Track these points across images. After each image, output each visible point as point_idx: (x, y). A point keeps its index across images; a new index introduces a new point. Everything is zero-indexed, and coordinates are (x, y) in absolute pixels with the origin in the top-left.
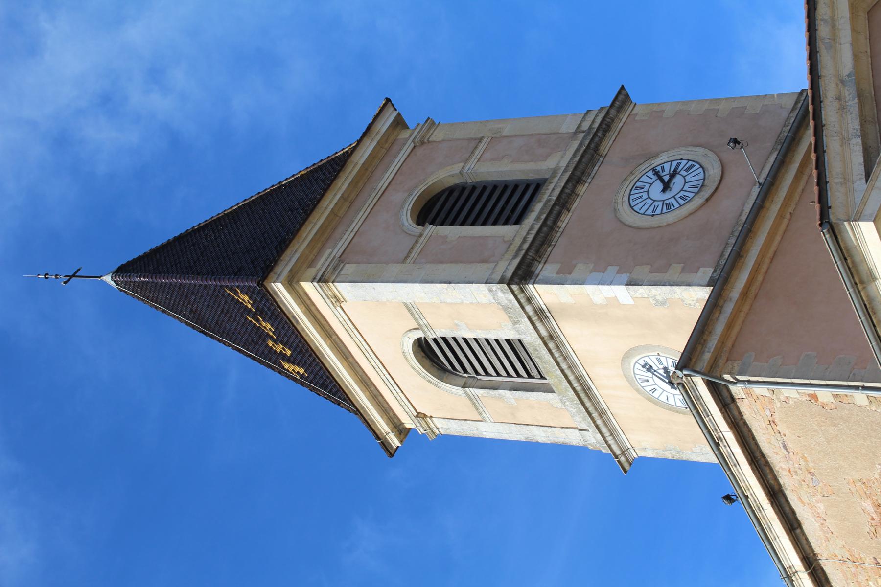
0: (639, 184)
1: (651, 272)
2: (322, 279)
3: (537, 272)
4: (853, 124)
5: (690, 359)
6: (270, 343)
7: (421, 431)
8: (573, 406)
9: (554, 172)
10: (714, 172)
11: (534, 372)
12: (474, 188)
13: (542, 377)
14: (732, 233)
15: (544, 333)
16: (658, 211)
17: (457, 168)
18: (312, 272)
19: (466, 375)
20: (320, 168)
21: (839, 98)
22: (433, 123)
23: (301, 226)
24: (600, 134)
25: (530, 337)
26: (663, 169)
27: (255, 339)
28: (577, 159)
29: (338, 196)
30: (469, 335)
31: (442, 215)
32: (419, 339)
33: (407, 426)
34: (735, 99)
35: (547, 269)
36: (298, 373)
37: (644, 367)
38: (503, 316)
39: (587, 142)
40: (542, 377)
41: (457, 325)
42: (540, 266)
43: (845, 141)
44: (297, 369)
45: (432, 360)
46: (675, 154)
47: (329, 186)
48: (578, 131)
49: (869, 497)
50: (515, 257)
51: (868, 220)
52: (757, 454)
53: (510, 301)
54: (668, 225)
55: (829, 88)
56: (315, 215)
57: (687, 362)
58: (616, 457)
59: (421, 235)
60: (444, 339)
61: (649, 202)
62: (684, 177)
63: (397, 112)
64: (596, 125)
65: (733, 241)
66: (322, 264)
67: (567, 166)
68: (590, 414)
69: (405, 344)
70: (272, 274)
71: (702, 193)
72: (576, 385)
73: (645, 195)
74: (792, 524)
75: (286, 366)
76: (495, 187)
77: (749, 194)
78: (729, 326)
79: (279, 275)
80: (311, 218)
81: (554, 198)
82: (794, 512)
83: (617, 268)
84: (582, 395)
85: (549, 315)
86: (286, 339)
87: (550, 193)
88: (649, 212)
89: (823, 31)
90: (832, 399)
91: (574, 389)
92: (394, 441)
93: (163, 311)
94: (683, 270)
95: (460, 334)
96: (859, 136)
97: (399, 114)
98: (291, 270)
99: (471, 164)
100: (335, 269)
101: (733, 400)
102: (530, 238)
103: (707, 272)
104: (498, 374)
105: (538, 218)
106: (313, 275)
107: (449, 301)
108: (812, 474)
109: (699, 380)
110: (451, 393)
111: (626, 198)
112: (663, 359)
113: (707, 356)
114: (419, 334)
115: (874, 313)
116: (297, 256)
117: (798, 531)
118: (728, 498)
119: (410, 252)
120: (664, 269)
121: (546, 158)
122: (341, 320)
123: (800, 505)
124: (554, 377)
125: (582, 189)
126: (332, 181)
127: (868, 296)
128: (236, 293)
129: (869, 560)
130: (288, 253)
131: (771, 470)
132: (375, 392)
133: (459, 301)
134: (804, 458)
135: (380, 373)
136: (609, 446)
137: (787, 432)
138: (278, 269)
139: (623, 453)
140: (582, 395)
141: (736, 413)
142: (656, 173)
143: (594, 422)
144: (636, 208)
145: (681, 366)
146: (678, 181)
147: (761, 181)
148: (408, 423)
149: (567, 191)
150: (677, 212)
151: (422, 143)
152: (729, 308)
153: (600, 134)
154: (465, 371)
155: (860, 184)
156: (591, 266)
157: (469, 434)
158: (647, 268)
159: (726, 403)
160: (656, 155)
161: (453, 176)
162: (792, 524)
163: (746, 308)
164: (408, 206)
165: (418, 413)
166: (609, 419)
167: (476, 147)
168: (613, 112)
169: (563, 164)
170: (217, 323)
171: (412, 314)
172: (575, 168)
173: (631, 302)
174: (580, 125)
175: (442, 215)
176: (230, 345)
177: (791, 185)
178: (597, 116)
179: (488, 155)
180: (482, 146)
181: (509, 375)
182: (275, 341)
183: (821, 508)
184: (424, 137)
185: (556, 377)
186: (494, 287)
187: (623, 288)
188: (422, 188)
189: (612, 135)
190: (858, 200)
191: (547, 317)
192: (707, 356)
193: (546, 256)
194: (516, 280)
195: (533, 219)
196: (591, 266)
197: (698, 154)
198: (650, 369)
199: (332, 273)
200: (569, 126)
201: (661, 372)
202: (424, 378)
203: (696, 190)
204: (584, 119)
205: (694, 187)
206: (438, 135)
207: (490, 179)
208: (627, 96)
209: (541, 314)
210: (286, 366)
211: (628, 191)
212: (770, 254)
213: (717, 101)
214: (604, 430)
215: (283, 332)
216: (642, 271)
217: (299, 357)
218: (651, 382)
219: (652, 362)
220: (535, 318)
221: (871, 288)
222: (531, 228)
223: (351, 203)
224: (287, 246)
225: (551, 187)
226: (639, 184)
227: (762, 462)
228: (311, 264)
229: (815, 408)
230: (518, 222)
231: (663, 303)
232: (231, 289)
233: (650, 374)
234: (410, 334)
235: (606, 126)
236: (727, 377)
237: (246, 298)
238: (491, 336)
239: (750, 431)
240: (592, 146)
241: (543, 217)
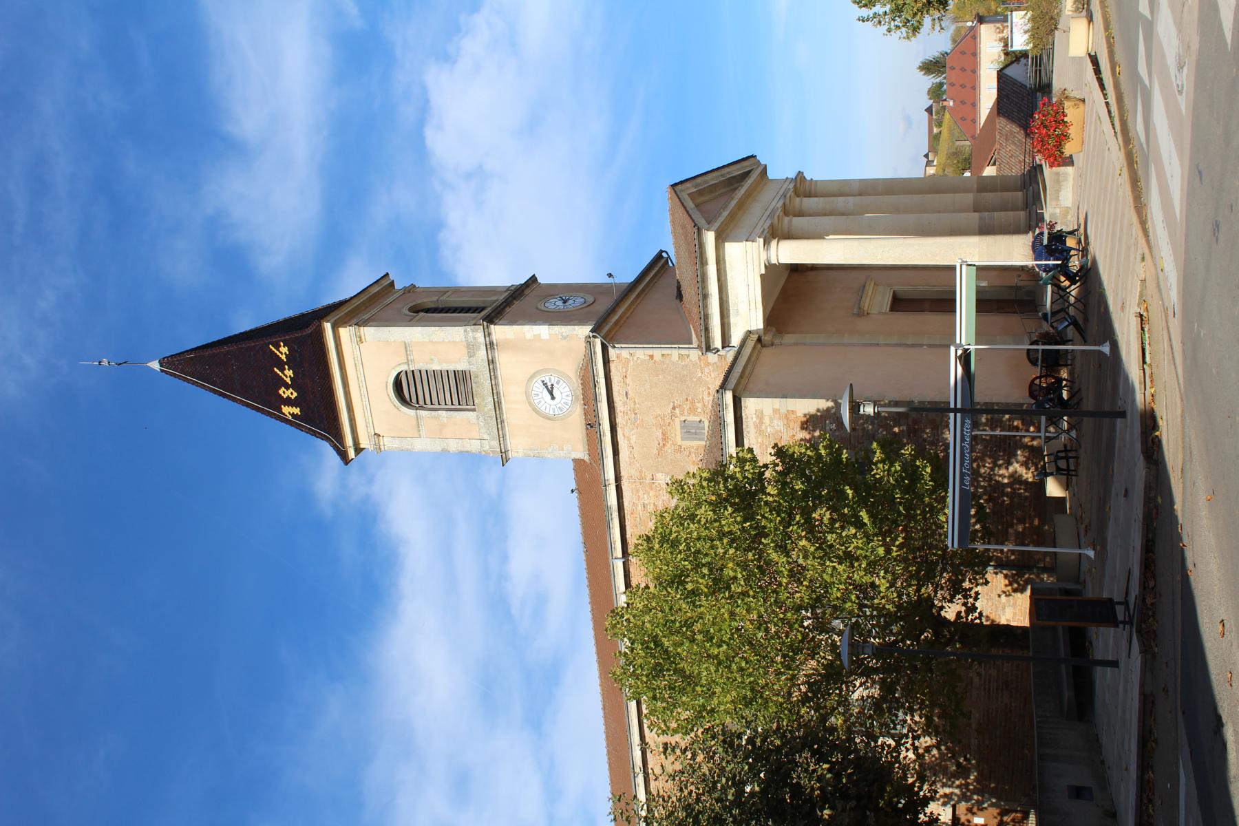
15: (490, 358)
17: (435, 299)
19: (417, 406)
29: (361, 301)
41: (432, 360)
72: (495, 397)
84: (497, 405)
85: (495, 347)
103: (594, 323)
112: (552, 378)
122: (355, 356)
123: (623, 438)
132: (352, 416)
133: (441, 340)
135: (364, 400)
140: (497, 405)
177: (633, 301)
183: (634, 439)
191: (494, 349)
219: (547, 380)
220: (488, 347)
231: (565, 338)
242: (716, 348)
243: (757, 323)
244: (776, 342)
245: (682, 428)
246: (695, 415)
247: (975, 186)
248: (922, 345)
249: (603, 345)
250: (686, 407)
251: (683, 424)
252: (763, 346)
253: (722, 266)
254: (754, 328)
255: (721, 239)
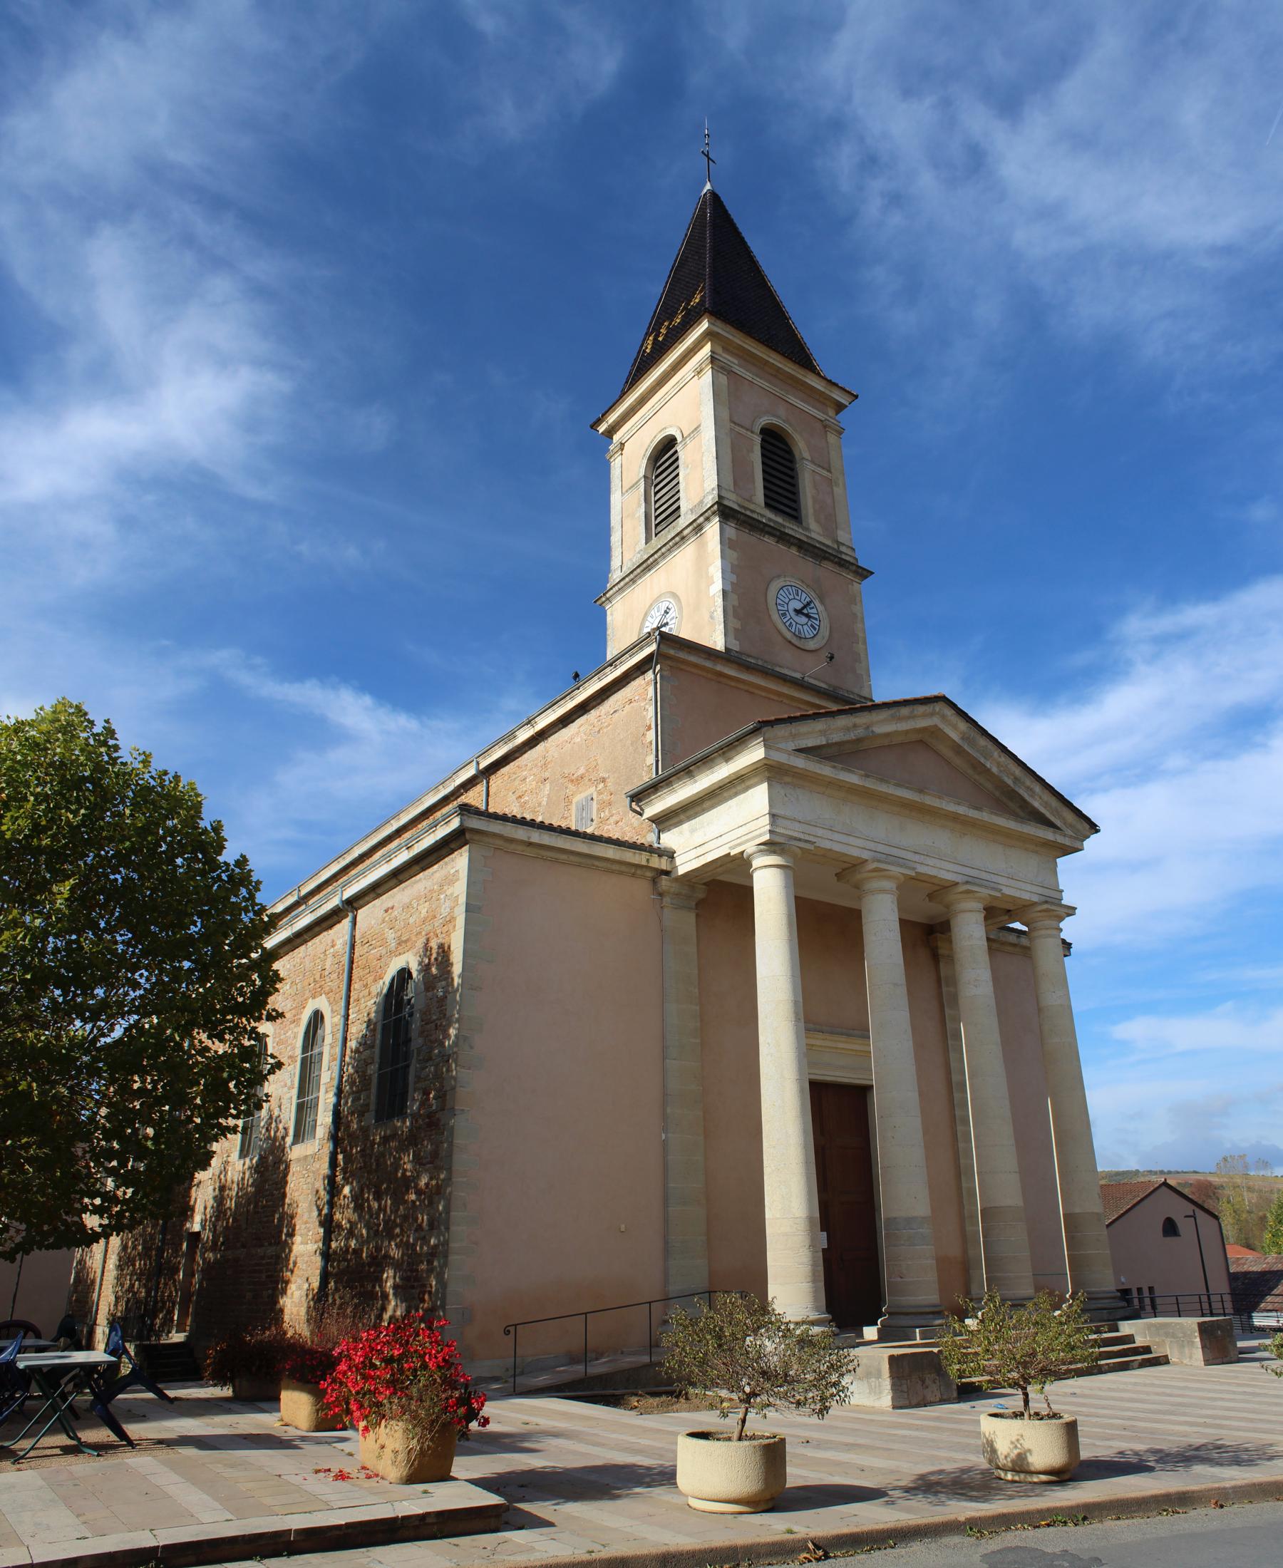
0: (800, 591)
1: (734, 606)
2: (713, 359)
3: (729, 523)
4: (836, 737)
5: (668, 640)
6: (666, 324)
7: (611, 447)
8: (638, 559)
9: (807, 529)
10: (812, 645)
11: (659, 528)
12: (792, 469)
13: (656, 535)
14: (766, 662)
15: (685, 532)
16: (780, 608)
17: (806, 455)
18: (719, 350)
20: (803, 348)
21: (855, 726)
22: (841, 433)
23: (754, 338)
24: (836, 559)
25: (682, 522)
26: (813, 608)
27: (669, 311)
28: (817, 545)
29: (779, 365)
30: (681, 477)
31: (770, 447)
32: (676, 439)
33: (614, 437)
34: (867, 655)
35: (731, 531)
36: (647, 348)
37: (667, 608)
38: (696, 501)
39: (830, 551)
40: (656, 535)
41: (688, 467)
42: (733, 525)
43: (823, 733)
44: (649, 347)
45: (662, 450)
46: (824, 615)
47: (787, 357)
48: (839, 543)
49: (587, 771)
50: (739, 505)
51: (766, 752)
52: (609, 693)
53: (706, 505)
54: (770, 616)
55: (862, 719)
56: (764, 349)
57: (666, 639)
58: (604, 594)
59: (752, 432)
60: (677, 459)
61: (787, 600)
62: (807, 624)
63: (847, 404)
64: (844, 557)
65: (760, 663)
66: (726, 358)
67: (812, 538)
68: (632, 572)
69: (670, 429)
70: (714, 318)
71: (795, 638)
72: (651, 560)
73: (791, 597)
74: (565, 721)
75: (651, 338)
76: (794, 485)
77: (795, 671)
78: (696, 666)
79: (714, 325)
80: (761, 345)
81: (786, 531)
82: (573, 722)
83: (735, 582)
84: (644, 565)
86: (670, 335)
87: (791, 528)
88: (779, 601)
89: (905, 711)
90: (648, 740)
91: (648, 559)
92: (602, 428)
93: (686, 235)
94: (736, 630)
95: (681, 471)
96: (827, 741)
97: (846, 406)
98: (718, 333)
99: (811, 466)
100: (722, 368)
101: (643, 673)
102: (755, 516)
103: (735, 646)
104: (656, 502)
105: (770, 520)
106: (716, 351)
107: (704, 459)
108: (599, 731)
109: (653, 647)
110: (640, 467)
111: (789, 584)
112: (673, 621)
113: (672, 652)
114: (679, 439)
115: (704, 763)
116: (730, 337)
117: (561, 726)
118: (576, 676)
119: (739, 425)
120: (736, 615)
121: (818, 521)
124: (656, 543)
125: (794, 551)
126: (791, 359)
127: (715, 758)
128: (701, 292)
129: (547, 775)
130: (733, 330)
131: (599, 704)
132: (636, 409)
133: (704, 466)
134: (609, 725)
136: (611, 589)
137: (625, 712)
138: (719, 323)
139: (608, 599)
140: (644, 565)
141: (634, 676)
142: (808, 604)
143: (627, 576)
144: (781, 592)
145: (662, 635)
146: (803, 620)
147: (806, 679)
148: (616, 438)
149: (792, 540)
150: (779, 621)
151: (825, 427)
152: (708, 664)
153: (836, 559)
154: (657, 477)
155: (791, 746)
156: (736, 563)
157: (613, 485)
158: (736, 603)
159: (640, 669)
160: (822, 602)
161: (801, 453)
162: (565, 721)
163: (709, 676)
164: (775, 421)
165: (624, 444)
166: (630, 586)
167: (824, 468)
168: (854, 568)
169: (813, 535)
170: (679, 279)
171: (693, 432)
172: (809, 544)
173: (711, 594)
174: (843, 544)
175: (770, 447)
176: (664, 291)
178: (851, 556)
179: (818, 478)
180: (825, 473)
181: (656, 510)
182: (668, 327)
183: (577, 740)
184: (830, 427)
185: (657, 545)
186: (716, 492)
187: (720, 587)
188: (790, 430)
189: (837, 569)
190: (780, 746)
191: (697, 533)
192: (672, 652)
193: (741, 528)
194: (721, 508)
195: (769, 516)
196: (736, 563)
197: (825, 632)
198: (666, 612)
199: (718, 366)
200: (842, 536)
201: (665, 621)
202: (649, 446)
203: (797, 633)
204: (849, 547)
205: (800, 632)
206: (832, 438)
207: (800, 481)
208: (866, 577)
209: (698, 528)
210: (651, 338)
211: (793, 584)
212: (751, 690)
213: (865, 643)
214: (622, 584)
215: (674, 333)
216: (734, 599)
217: (657, 347)
218: (658, 614)
219: (672, 614)
220: (695, 525)
221: (720, 759)
222: (763, 516)
223: (775, 376)
224: (737, 328)
225: (796, 529)
226: (800, 591)
227: (604, 697)
228: (725, 349)
229: (642, 730)
230: (767, 505)
231: (712, 617)
232: (703, 288)
233: (663, 612)
234: (679, 432)
235: (842, 563)
236: (658, 667)
237: (697, 301)
238: (681, 494)
239: (624, 686)
240: (827, 555)
241: (772, 524)
242: (643, 810)
243: (685, 864)
244: (667, 900)
245: (586, 798)
246: (598, 810)
247: (1077, 1210)
248: (665, 1130)
249: (650, 657)
250: (605, 797)
251: (589, 798)
252: (654, 881)
253: (739, 788)
254: (678, 861)
255: (770, 771)
